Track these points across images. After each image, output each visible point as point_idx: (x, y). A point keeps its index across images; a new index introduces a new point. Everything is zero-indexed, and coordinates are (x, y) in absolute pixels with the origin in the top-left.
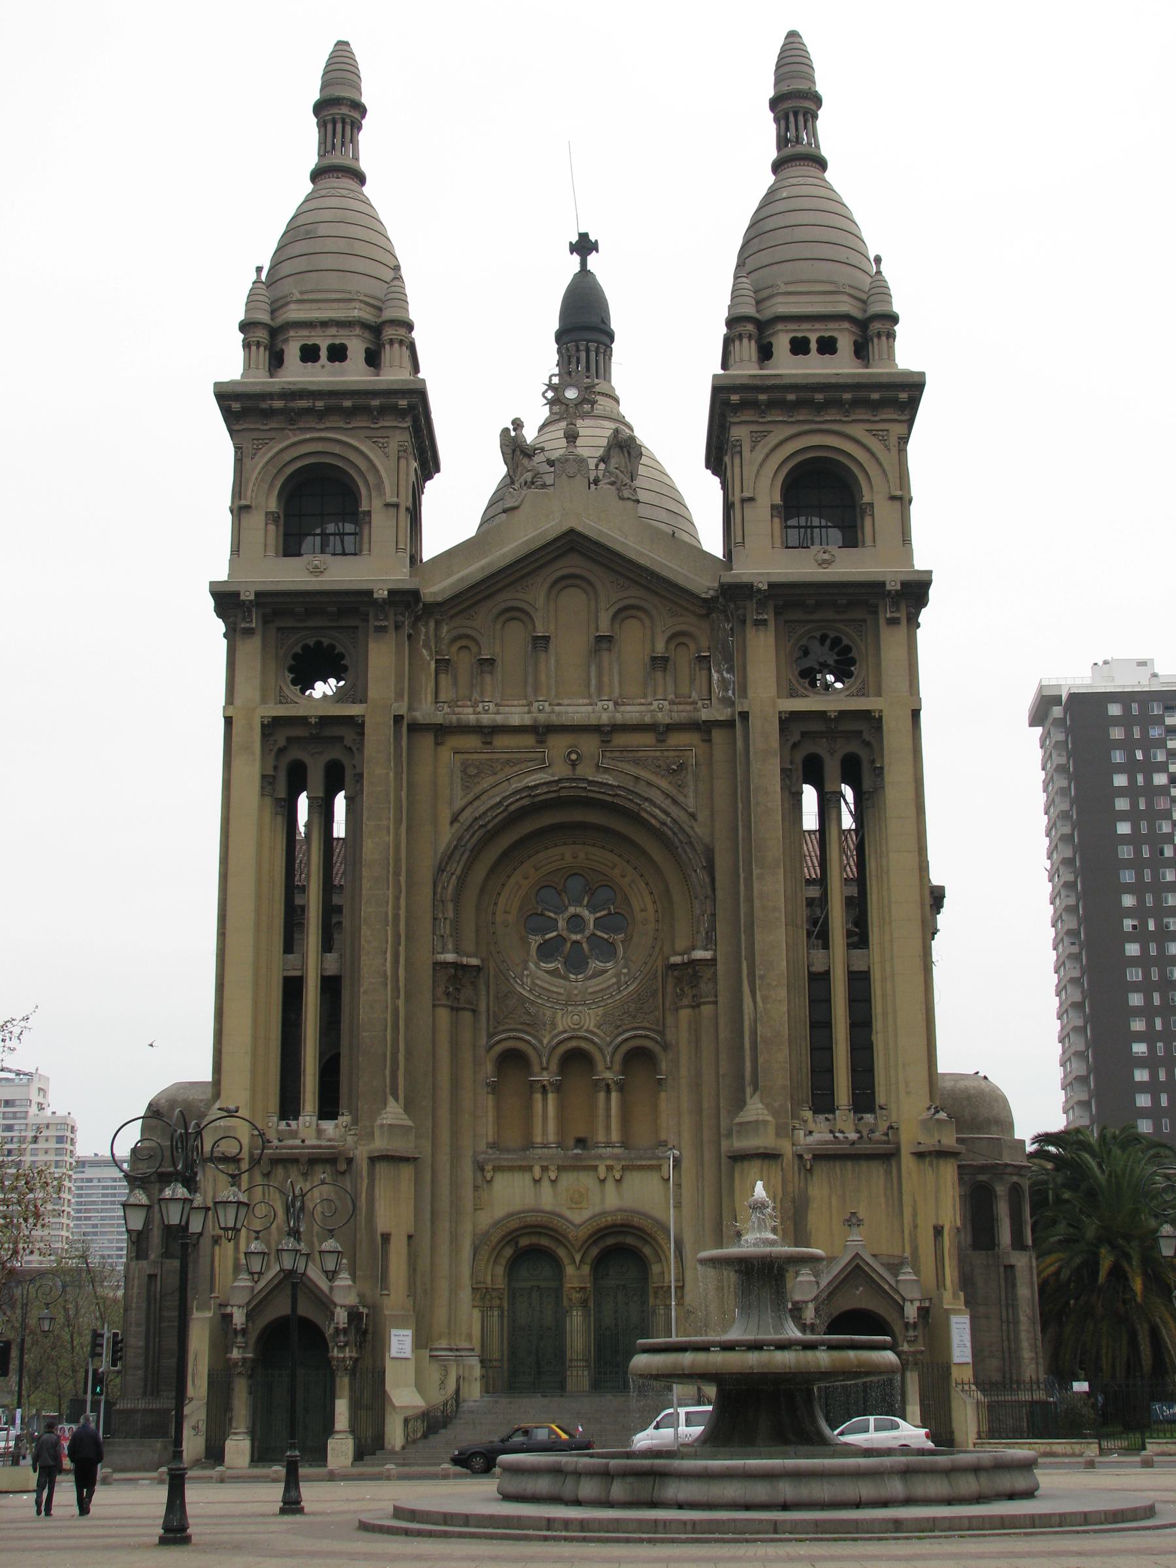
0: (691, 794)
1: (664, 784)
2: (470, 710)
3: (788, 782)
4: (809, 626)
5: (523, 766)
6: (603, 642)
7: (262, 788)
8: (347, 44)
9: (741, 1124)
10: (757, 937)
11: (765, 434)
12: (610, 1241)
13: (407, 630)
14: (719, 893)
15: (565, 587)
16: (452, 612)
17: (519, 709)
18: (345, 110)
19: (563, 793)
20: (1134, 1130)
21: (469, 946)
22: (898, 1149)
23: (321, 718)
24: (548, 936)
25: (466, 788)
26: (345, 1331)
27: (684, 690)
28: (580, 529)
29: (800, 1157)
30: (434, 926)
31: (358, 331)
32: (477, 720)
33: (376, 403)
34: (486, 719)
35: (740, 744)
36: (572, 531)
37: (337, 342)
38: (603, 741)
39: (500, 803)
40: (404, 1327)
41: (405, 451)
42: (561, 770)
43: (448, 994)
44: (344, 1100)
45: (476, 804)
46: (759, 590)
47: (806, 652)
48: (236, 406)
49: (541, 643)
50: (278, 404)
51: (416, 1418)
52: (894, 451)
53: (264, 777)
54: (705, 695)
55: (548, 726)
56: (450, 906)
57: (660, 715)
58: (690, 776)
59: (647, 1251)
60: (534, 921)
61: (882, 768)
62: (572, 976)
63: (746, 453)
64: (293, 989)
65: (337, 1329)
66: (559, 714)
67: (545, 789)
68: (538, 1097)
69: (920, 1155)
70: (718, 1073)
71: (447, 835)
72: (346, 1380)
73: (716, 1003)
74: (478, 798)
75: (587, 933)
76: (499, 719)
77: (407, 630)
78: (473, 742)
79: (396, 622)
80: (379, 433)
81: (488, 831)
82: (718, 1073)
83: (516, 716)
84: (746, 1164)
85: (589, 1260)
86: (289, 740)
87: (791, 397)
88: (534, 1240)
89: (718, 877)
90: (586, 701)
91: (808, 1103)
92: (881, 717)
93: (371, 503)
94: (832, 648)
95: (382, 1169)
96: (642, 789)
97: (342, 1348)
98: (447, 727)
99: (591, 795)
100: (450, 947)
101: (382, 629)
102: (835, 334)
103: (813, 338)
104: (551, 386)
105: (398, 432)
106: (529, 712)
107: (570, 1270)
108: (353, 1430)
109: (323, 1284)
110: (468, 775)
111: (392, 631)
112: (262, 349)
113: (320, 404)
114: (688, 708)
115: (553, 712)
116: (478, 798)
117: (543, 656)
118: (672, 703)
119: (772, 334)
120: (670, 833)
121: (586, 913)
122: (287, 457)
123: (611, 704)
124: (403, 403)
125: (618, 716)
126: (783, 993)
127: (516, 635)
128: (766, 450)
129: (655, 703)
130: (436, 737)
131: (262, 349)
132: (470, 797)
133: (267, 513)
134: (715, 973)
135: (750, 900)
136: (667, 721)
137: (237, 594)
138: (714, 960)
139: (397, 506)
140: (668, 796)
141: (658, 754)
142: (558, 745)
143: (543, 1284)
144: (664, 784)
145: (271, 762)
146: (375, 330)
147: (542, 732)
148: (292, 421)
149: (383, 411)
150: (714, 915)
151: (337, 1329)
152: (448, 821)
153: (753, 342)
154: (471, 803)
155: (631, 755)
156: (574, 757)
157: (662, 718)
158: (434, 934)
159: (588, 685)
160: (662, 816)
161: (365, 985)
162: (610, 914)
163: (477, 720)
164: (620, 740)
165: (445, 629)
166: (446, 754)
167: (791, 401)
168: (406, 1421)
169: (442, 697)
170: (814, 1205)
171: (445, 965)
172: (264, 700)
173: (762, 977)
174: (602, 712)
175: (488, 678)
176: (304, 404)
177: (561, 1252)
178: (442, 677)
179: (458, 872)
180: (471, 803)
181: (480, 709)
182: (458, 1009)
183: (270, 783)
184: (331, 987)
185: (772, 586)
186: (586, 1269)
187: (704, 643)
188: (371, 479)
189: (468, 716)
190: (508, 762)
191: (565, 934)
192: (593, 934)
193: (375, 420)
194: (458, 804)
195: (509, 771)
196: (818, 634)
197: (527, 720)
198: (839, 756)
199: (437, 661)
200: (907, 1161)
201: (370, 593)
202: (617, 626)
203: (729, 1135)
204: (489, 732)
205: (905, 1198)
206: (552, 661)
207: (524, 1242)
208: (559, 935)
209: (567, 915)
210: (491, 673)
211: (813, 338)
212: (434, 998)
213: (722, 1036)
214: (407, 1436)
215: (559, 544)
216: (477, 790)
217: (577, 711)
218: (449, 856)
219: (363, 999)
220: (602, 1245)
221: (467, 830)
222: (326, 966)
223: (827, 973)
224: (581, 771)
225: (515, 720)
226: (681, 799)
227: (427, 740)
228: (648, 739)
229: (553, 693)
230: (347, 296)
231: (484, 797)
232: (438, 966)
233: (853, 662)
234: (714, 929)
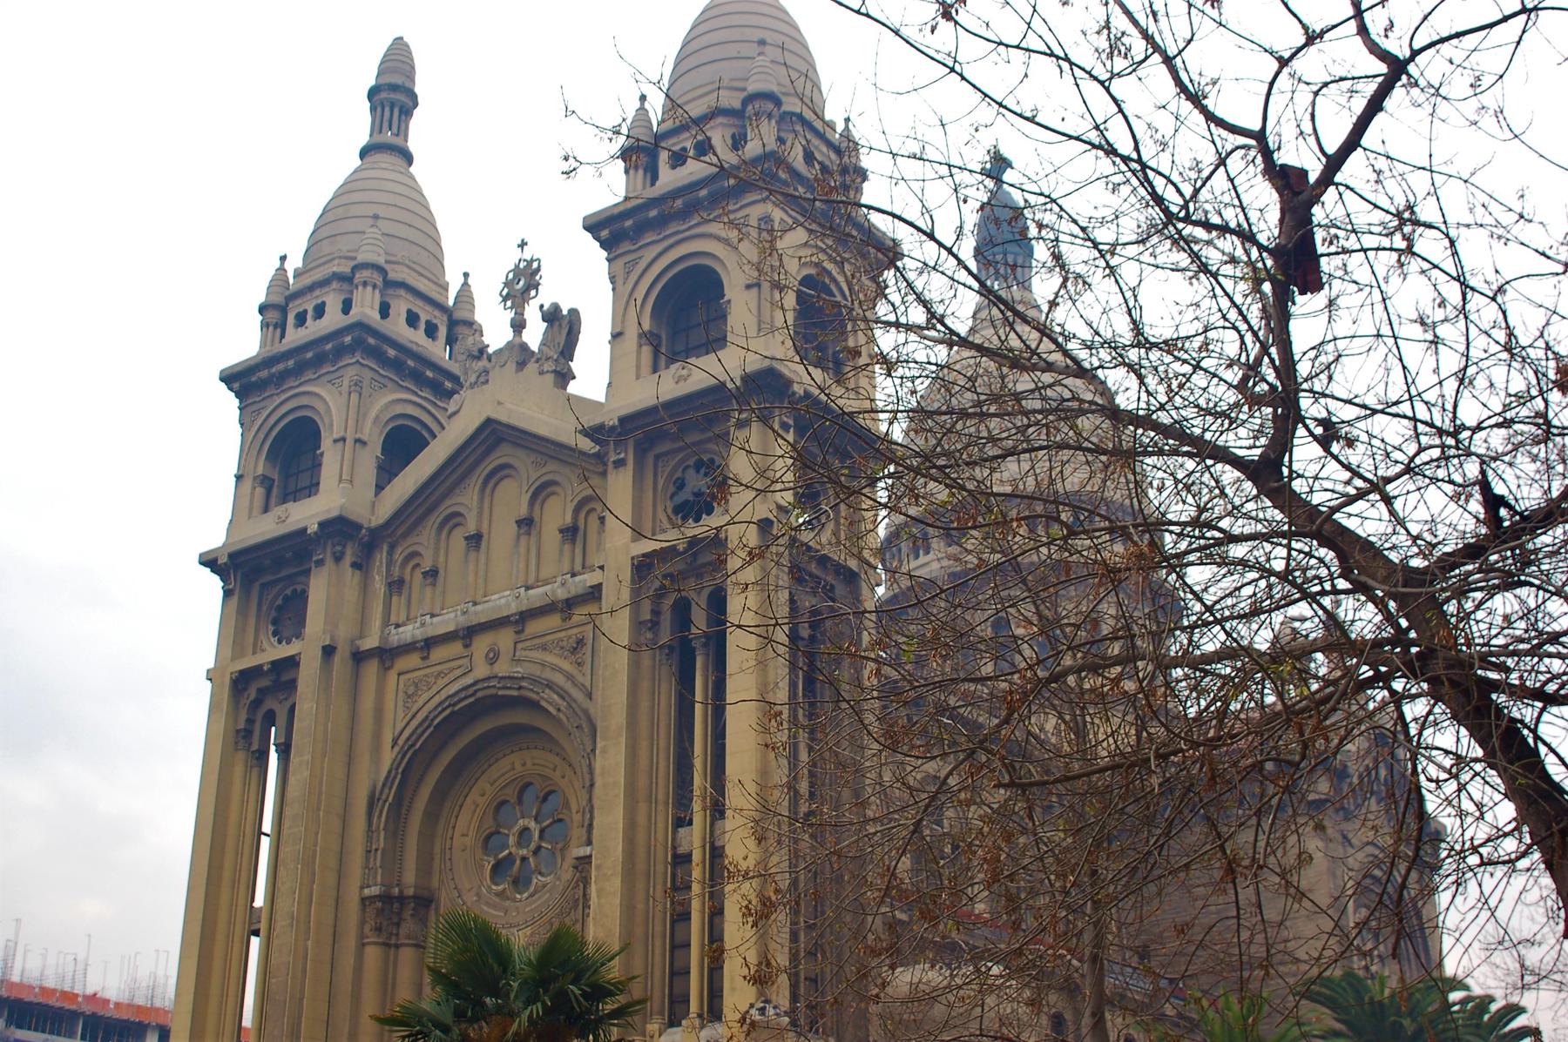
1: (566, 665)
3: (649, 635)
4: (681, 456)
5: (452, 676)
7: (236, 743)
8: (401, 38)
11: (635, 262)
13: (348, 558)
16: (400, 531)
18: (384, 95)
19: (480, 694)
20: (1494, 1007)
21: (410, 877)
23: (273, 663)
24: (501, 856)
28: (494, 416)
30: (367, 859)
31: (335, 285)
32: (413, 636)
33: (329, 346)
36: (489, 422)
37: (319, 301)
38: (516, 633)
41: (356, 385)
42: (481, 671)
43: (378, 929)
46: (613, 428)
47: (681, 485)
48: (236, 386)
49: (475, 540)
50: (264, 374)
53: (238, 731)
55: (468, 628)
60: (489, 841)
62: (518, 896)
67: (463, 695)
74: (414, 716)
75: (533, 846)
77: (348, 558)
78: (413, 660)
79: (334, 553)
80: (337, 375)
81: (416, 752)
83: (447, 622)
86: (260, 690)
87: (653, 213)
91: (661, 1013)
93: (326, 444)
96: (548, 675)
98: (391, 650)
99: (500, 693)
101: (320, 563)
104: (506, 284)
105: (350, 368)
111: (330, 564)
112: (271, 328)
113: (291, 363)
116: (414, 716)
117: (473, 555)
120: (564, 719)
121: (532, 825)
122: (272, 421)
124: (348, 339)
126: (617, 882)
127: (458, 540)
128: (635, 278)
130: (382, 662)
131: (271, 328)
133: (255, 478)
136: (566, 596)
137: (216, 560)
139: (344, 439)
140: (569, 677)
141: (563, 634)
142: (481, 644)
144: (566, 665)
145: (243, 716)
146: (347, 279)
147: (468, 634)
148: (278, 385)
149: (340, 352)
153: (641, 172)
155: (536, 641)
157: (562, 594)
160: (559, 701)
162: (554, 822)
163: (413, 636)
164: (534, 627)
165: (399, 550)
166: (392, 676)
167: (655, 218)
169: (393, 619)
171: (372, 898)
172: (233, 659)
175: (429, 590)
176: (281, 367)
178: (395, 599)
182: (397, 946)
183: (244, 737)
185: (623, 420)
188: (327, 420)
189: (409, 632)
190: (439, 675)
191: (513, 850)
192: (539, 848)
193: (334, 362)
194: (400, 726)
195: (441, 683)
196: (691, 462)
198: (706, 593)
199: (390, 585)
201: (305, 529)
202: (537, 507)
208: (510, 853)
209: (516, 829)
210: (434, 585)
212: (362, 936)
215: (483, 437)
216: (414, 709)
223: (690, 855)
226: (580, 679)
227: (371, 669)
228: (554, 621)
229: (481, 592)
230: (329, 258)
232: (364, 901)
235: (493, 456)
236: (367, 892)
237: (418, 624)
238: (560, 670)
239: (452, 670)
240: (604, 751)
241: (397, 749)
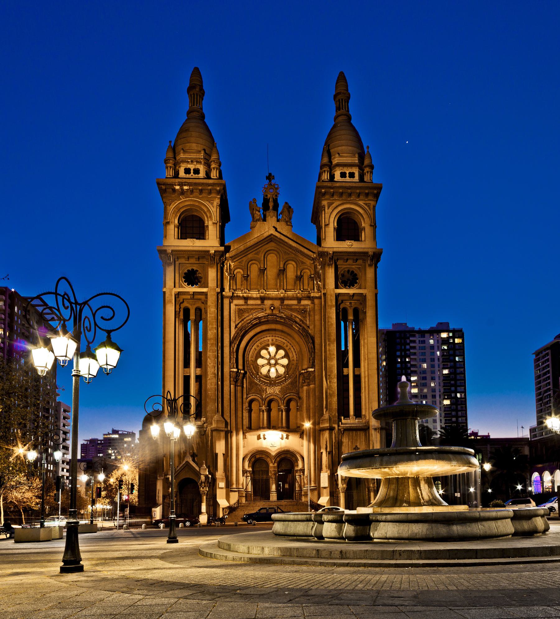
0: (308, 320)
2: (241, 292)
6: (282, 272)
9: (322, 420)
10: (328, 363)
12: (283, 456)
14: (316, 351)
15: (268, 254)
17: (255, 292)
22: (369, 428)
25: (239, 317)
26: (204, 483)
27: (306, 287)
29: (340, 430)
34: (245, 295)
35: (323, 303)
39: (250, 322)
40: (222, 482)
42: (269, 312)
44: (203, 414)
45: (242, 322)
51: (226, 508)
52: (372, 211)
54: (312, 288)
56: (235, 354)
57: (299, 295)
58: (307, 315)
59: (294, 459)
61: (366, 312)
63: (326, 210)
64: (187, 379)
65: (202, 482)
66: (268, 294)
68: (261, 413)
69: (375, 429)
70: (315, 405)
71: (233, 331)
72: (205, 497)
73: (315, 384)
74: (243, 320)
76: (250, 295)
78: (241, 302)
82: (315, 405)
84: (324, 432)
85: (276, 461)
88: (261, 456)
89: (316, 346)
90: (276, 290)
92: (366, 296)
94: (351, 275)
95: (214, 433)
97: (203, 488)
100: (235, 367)
102: (354, 172)
103: (347, 172)
106: (259, 293)
107: (271, 465)
108: (207, 512)
109: (197, 469)
110: (240, 312)
114: (307, 293)
115: (266, 293)
118: (302, 291)
119: (335, 171)
123: (284, 291)
125: (286, 295)
126: (335, 380)
129: (297, 291)
132: (241, 319)
134: (315, 375)
135: (325, 352)
138: (314, 371)
140: (301, 320)
142: (268, 303)
143: (263, 469)
144: (300, 317)
147: (263, 299)
150: (314, 357)
151: (202, 482)
152: (234, 327)
154: (241, 322)
156: (272, 308)
158: (230, 362)
159: (277, 285)
161: (209, 377)
163: (243, 296)
164: (286, 302)
168: (223, 509)
170: (344, 444)
173: (329, 375)
174: (281, 293)
177: (268, 460)
178: (231, 281)
179: (237, 343)
180: (241, 322)
181: (243, 292)
184: (199, 378)
186: (276, 465)
187: (313, 273)
190: (252, 309)
194: (237, 323)
197: (258, 296)
200: (372, 432)
203: (319, 424)
204: (246, 299)
205: (370, 442)
206: (266, 278)
207: (258, 456)
211: (347, 172)
213: (317, 394)
214: (223, 514)
217: (273, 293)
218: (235, 338)
219: (208, 381)
220: (280, 457)
221: (240, 330)
222: (197, 372)
224: (274, 312)
225: (255, 296)
228: (295, 302)
231: (245, 320)
233: (358, 279)
234: (315, 362)
235: (267, 246)
236: (232, 370)
237: (243, 292)
238: (298, 318)
239: (256, 309)
240: (329, 345)
241: (237, 329)
